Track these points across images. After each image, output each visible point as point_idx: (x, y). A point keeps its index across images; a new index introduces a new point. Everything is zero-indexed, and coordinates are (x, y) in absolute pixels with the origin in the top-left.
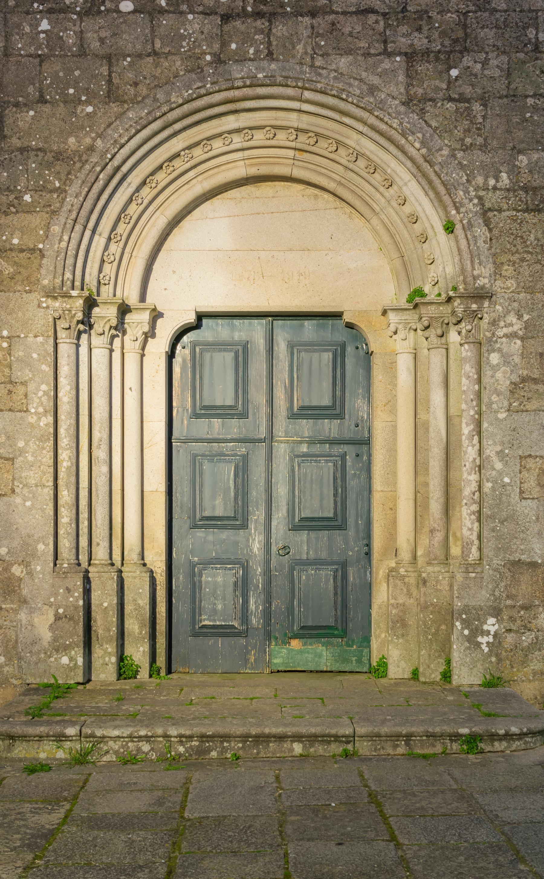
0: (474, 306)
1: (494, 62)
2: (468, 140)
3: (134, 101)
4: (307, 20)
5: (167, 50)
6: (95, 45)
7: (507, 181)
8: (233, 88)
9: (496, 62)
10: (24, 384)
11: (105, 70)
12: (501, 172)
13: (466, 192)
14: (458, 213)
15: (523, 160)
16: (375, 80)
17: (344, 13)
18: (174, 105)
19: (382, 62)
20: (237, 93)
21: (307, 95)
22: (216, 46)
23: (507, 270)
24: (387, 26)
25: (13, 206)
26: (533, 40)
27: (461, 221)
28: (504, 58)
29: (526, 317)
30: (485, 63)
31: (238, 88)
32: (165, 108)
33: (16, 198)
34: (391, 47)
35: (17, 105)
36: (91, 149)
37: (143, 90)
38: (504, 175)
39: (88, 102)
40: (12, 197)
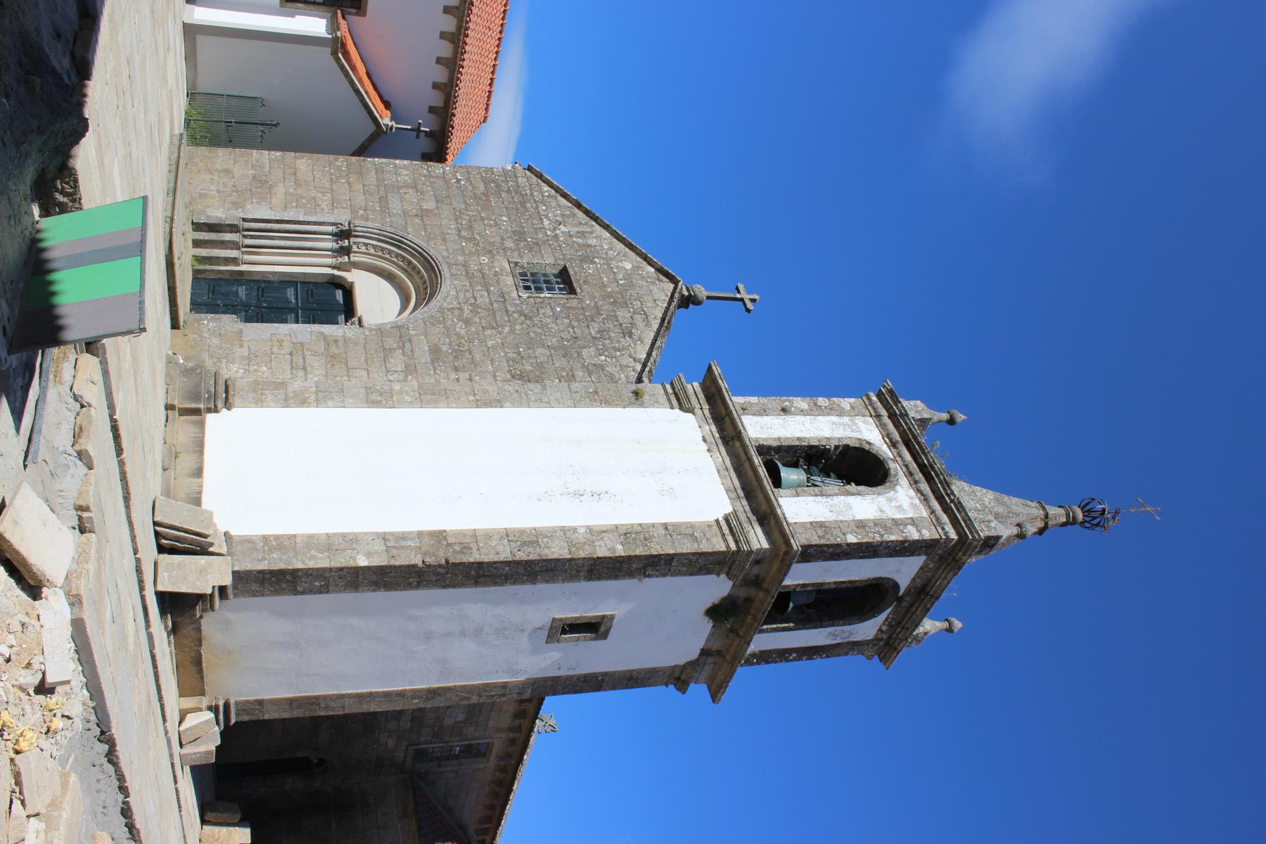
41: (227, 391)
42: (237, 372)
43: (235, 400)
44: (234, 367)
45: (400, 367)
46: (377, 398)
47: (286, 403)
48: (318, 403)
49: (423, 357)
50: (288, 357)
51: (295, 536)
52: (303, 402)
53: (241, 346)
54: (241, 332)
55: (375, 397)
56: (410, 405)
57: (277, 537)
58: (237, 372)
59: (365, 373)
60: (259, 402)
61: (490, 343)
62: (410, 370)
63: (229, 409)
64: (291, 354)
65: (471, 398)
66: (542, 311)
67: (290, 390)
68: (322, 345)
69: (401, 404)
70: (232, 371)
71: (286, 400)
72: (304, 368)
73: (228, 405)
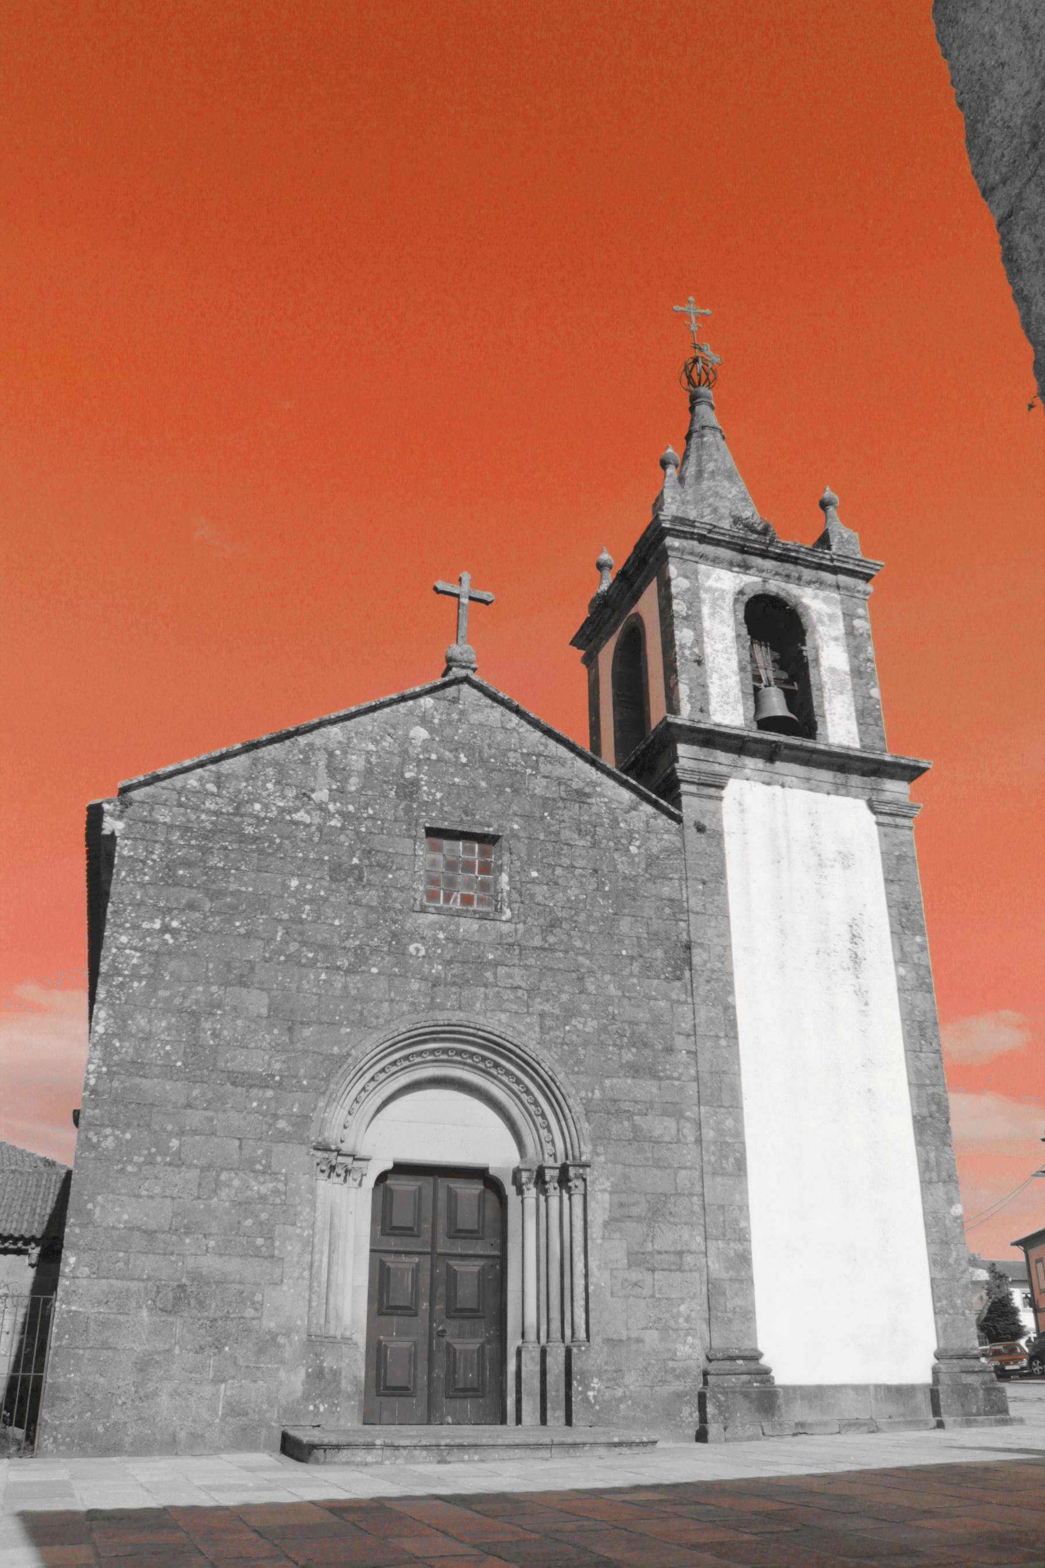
0: (581, 1171)
1: (589, 1024)
2: (576, 1069)
3: (377, 1028)
4: (482, 989)
6: (354, 992)
13: (575, 1100)
15: (607, 1082)
16: (523, 1029)
17: (505, 988)
22: (428, 1000)
23: (601, 1150)
24: (529, 997)
28: (595, 1022)
29: (612, 1179)
30: (585, 1024)
32: (396, 1034)
34: (531, 1009)
35: (302, 1023)
36: (349, 1055)
37: (381, 1021)
38: (597, 1092)
39: (346, 1026)
40: (294, 1081)
41: (732, 1359)
42: (692, 1346)
43: (746, 1344)
44: (682, 1350)
45: (670, 1124)
46: (733, 1162)
47: (747, 1282)
48: (743, 1237)
49: (647, 1088)
50: (658, 1275)
51: (933, 1280)
52: (744, 1259)
53: (639, 1341)
54: (609, 1341)
55: (729, 1165)
56: (739, 1120)
57: (936, 1298)
58: (692, 1346)
59: (683, 1173)
60: (748, 1315)
61: (612, 990)
62: (674, 1111)
63: (761, 1355)
64: (653, 1270)
65: (723, 1042)
66: (539, 899)
67: (724, 1275)
68: (630, 1225)
69: (738, 1134)
70: (690, 1351)
71: (741, 1282)
72: (680, 1254)
73: (755, 1357)
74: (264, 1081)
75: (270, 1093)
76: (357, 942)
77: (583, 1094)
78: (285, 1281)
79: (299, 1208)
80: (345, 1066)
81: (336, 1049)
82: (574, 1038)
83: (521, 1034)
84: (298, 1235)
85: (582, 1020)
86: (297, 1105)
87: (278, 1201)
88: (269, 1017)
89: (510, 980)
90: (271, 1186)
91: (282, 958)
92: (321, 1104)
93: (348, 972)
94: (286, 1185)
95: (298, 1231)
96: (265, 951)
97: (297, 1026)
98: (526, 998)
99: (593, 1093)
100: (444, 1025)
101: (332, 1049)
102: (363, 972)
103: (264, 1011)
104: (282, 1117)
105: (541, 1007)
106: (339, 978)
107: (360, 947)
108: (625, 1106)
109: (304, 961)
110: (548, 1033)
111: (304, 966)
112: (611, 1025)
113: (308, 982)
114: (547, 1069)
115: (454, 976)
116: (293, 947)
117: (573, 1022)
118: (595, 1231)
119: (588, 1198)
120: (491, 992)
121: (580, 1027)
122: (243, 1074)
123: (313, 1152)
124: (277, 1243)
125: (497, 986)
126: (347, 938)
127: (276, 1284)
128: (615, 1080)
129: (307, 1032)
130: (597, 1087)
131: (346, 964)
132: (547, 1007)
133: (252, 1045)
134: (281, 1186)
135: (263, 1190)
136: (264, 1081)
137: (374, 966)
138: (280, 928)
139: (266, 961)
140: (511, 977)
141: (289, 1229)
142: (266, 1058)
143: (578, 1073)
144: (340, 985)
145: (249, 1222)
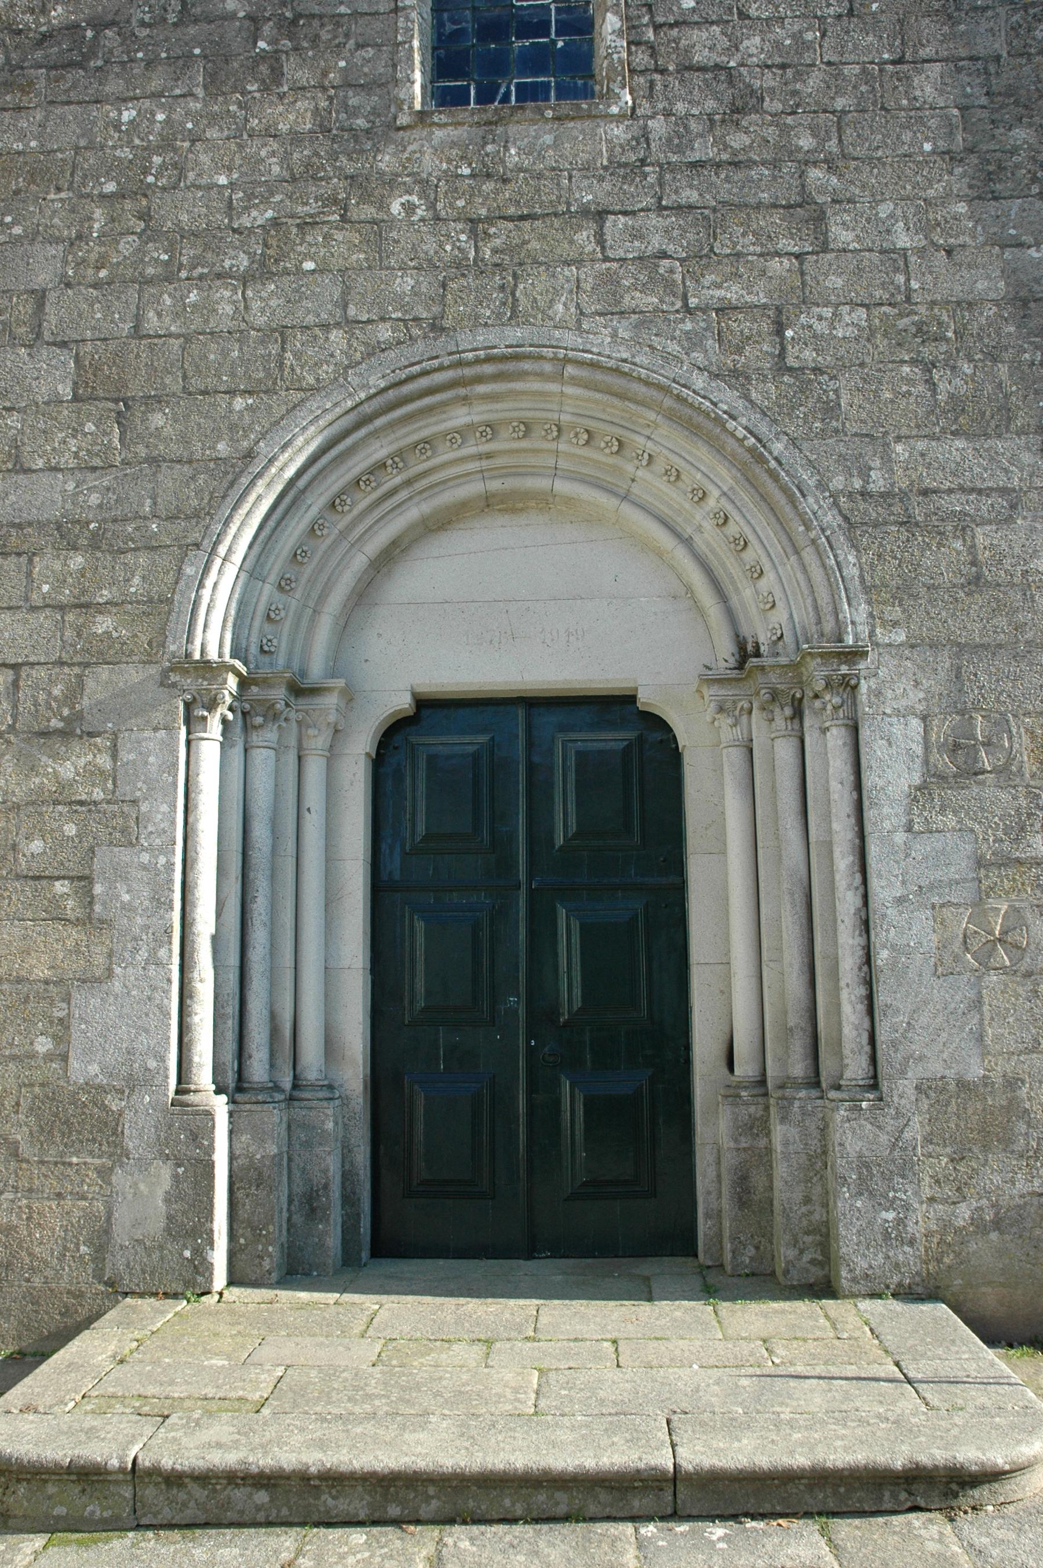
0: (844, 669)
5: (364, 318)
7: (881, 482)
8: (460, 364)
9: (847, 319)
10: (134, 802)
11: (274, 349)
12: (870, 469)
14: (808, 528)
16: (673, 347)
18: (372, 391)
19: (683, 320)
20: (468, 372)
21: (570, 370)
25: (132, 540)
26: (903, 288)
27: (813, 542)
31: (469, 364)
33: (136, 529)
74: (66, 534)
75: (77, 561)
76: (270, 214)
77: (838, 482)
78: (118, 970)
79: (144, 807)
80: (245, 481)
81: (222, 448)
82: (809, 355)
83: (668, 358)
84: (144, 868)
85: (827, 312)
86: (136, 580)
87: (98, 794)
88: (76, 398)
89: (637, 244)
90: (82, 762)
91: (103, 273)
92: (189, 570)
93: (245, 280)
94: (114, 757)
95: (145, 858)
96: (65, 262)
97: (138, 410)
98: (678, 277)
99: (866, 478)
100: (478, 361)
101: (213, 448)
102: (286, 272)
103: (65, 391)
104: (100, 609)
105: (719, 293)
106: (227, 294)
107: (275, 222)
108: (955, 503)
109: (150, 271)
110: (739, 350)
111: (149, 281)
112: (901, 315)
113: (159, 315)
114: (741, 432)
115: (495, 251)
116: (127, 245)
117: (803, 319)
118: (886, 817)
119: (865, 733)
120: (587, 275)
121: (820, 327)
122: (20, 526)
123: (174, 677)
124: (98, 889)
125: (606, 259)
126: (247, 209)
127: (99, 980)
128: (921, 445)
129: (158, 420)
130: (877, 463)
131: (244, 261)
132: (732, 293)
133: (40, 463)
134: (104, 761)
135: (67, 770)
136: (66, 534)
137: (308, 256)
138: (98, 213)
139: (68, 285)
140: (637, 235)
141: (124, 855)
142: (71, 486)
143: (823, 434)
144: (229, 309)
145: (37, 846)
